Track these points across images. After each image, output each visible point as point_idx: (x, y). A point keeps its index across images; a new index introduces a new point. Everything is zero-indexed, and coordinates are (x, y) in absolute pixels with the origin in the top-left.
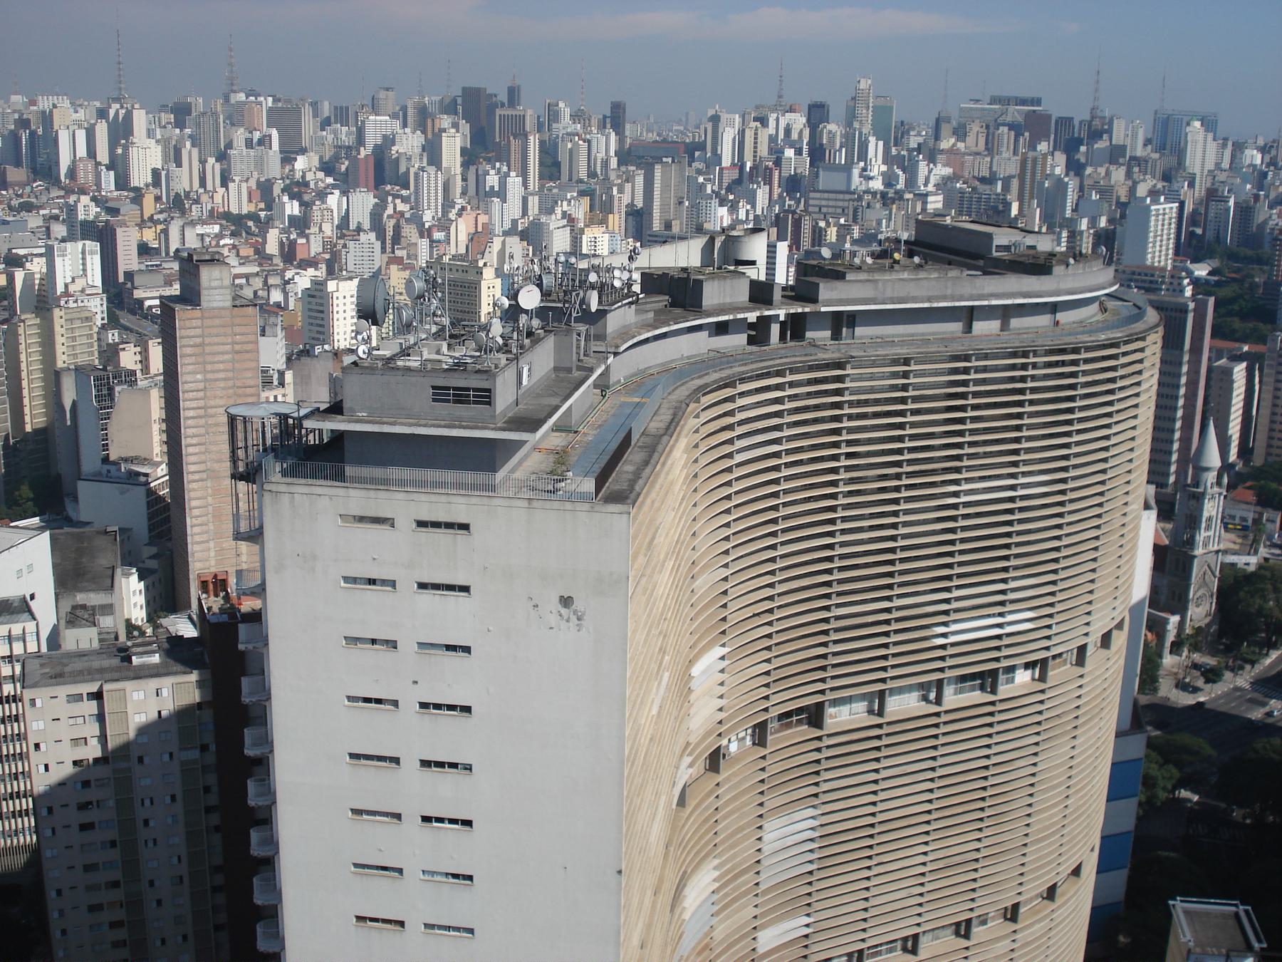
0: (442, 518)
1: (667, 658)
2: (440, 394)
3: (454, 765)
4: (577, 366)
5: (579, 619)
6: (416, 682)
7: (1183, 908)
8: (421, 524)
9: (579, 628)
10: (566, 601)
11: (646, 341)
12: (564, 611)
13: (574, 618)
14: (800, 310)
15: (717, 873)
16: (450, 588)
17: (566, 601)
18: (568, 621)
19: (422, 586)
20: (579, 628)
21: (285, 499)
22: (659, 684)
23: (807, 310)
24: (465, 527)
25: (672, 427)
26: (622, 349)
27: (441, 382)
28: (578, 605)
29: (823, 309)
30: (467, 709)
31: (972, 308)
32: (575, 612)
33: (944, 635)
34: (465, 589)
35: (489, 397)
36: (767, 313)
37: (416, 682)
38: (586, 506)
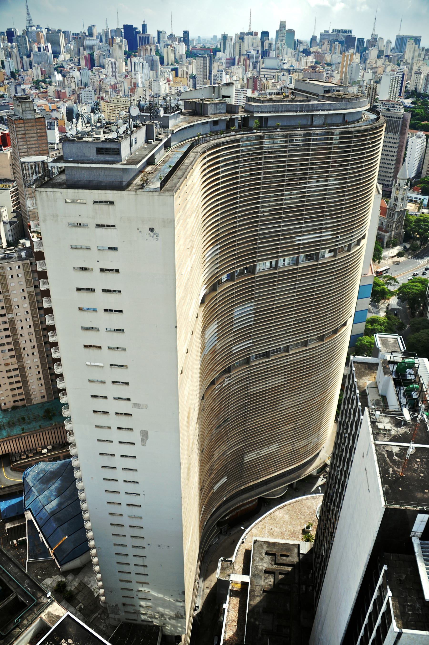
0: (104, 199)
1: (194, 250)
2: (100, 151)
3: (114, 291)
4: (156, 139)
5: (157, 236)
6: (98, 261)
7: (379, 337)
8: (96, 202)
9: (157, 239)
10: (152, 230)
11: (186, 128)
12: (151, 234)
13: (155, 236)
14: (246, 116)
15: (217, 326)
16: (108, 226)
17: (152, 230)
18: (153, 237)
19: (98, 225)
20: (157, 239)
21: (44, 194)
22: (191, 259)
23: (249, 116)
24: (112, 203)
25: (194, 162)
26: (175, 132)
27: (100, 146)
28: (156, 231)
29: (255, 115)
30: (117, 271)
31: (313, 115)
32: (155, 234)
33: (300, 240)
34: (114, 226)
35: (119, 152)
36: (233, 117)
37: (98, 261)
38: (157, 193)
